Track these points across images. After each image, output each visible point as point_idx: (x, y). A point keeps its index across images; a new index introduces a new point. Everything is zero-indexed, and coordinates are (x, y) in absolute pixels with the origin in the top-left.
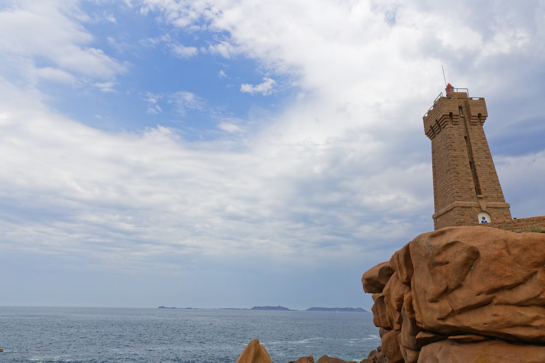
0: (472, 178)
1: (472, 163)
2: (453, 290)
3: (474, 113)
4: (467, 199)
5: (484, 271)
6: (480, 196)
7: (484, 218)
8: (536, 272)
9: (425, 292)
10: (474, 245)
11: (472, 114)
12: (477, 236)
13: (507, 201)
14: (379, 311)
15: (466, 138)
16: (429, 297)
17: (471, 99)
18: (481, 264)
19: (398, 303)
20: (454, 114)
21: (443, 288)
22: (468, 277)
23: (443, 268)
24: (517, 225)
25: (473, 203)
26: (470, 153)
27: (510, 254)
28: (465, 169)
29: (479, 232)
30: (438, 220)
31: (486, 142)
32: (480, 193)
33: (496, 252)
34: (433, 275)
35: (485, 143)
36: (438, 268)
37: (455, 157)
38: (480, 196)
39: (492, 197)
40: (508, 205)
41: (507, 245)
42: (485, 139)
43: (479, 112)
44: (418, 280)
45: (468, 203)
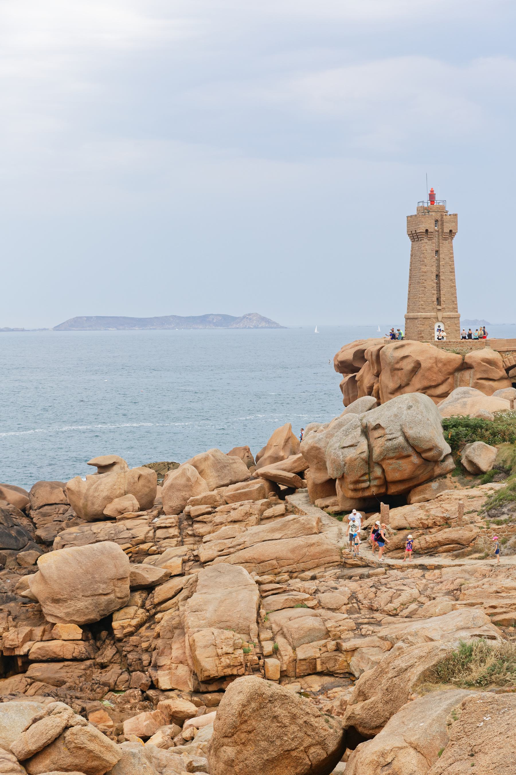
0: (435, 292)
1: (438, 276)
2: (404, 387)
3: (446, 230)
4: (429, 310)
5: (422, 376)
6: (439, 307)
7: (439, 326)
8: (449, 378)
9: (387, 387)
10: (419, 359)
11: (445, 231)
12: (422, 352)
13: (460, 312)
14: (350, 392)
15: (437, 252)
16: (389, 391)
17: (447, 212)
18: (421, 372)
19: (369, 390)
20: (429, 230)
21: (398, 386)
22: (414, 378)
23: (399, 373)
25: (433, 314)
26: (438, 266)
27: (437, 366)
28: (431, 283)
30: (408, 321)
31: (453, 257)
32: (440, 305)
33: (430, 365)
34: (393, 376)
35: (451, 258)
36: (396, 372)
37: (425, 272)
38: (439, 307)
39: (449, 308)
40: (459, 315)
41: (437, 361)
42: (452, 253)
43: (450, 229)
44: (385, 377)
45: (428, 314)
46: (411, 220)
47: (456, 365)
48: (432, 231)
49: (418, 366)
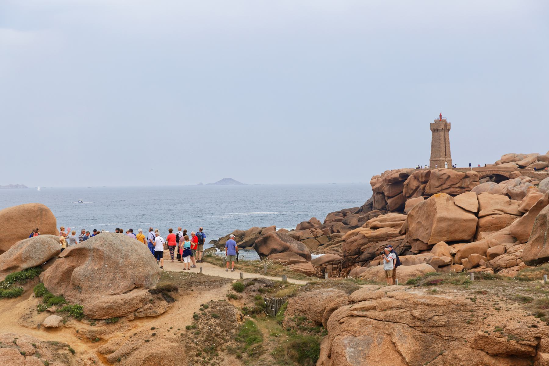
24: (458, 170)
25: (444, 159)
28: (443, 148)
29: (446, 170)
41: (456, 175)
46: (432, 125)
47: (463, 176)
48: (440, 129)
49: (449, 176)
